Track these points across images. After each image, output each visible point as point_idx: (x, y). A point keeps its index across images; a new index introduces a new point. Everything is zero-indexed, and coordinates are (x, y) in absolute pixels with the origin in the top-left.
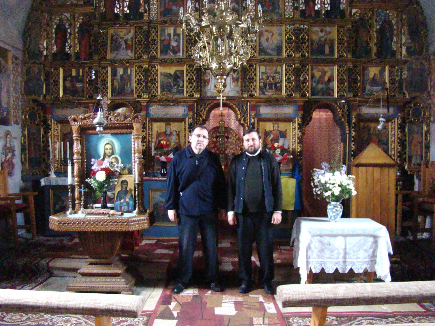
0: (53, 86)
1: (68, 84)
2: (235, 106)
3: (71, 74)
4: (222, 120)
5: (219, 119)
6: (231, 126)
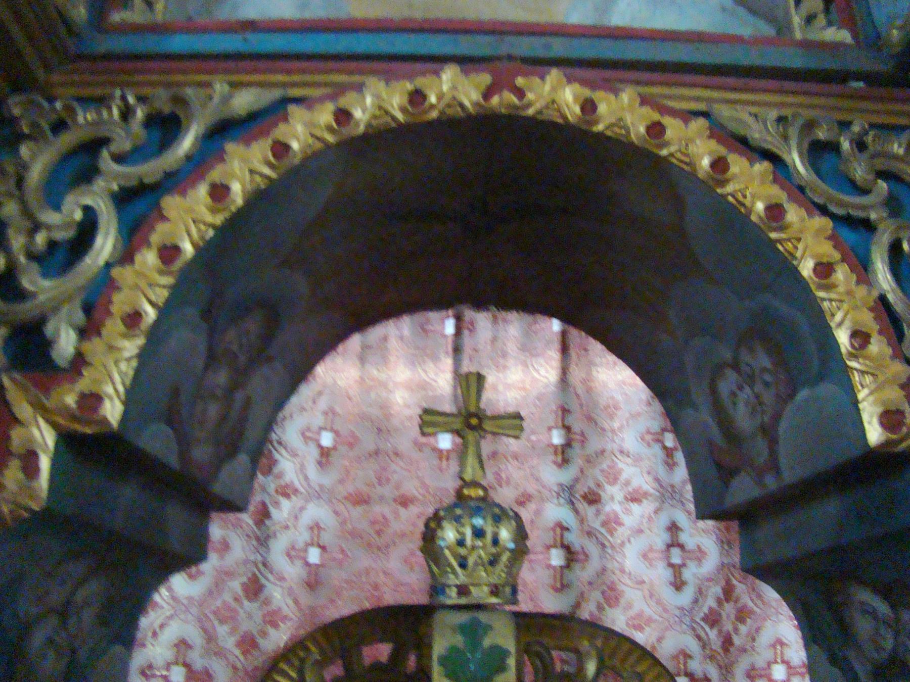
2: (751, 187)
4: (469, 501)
5: (429, 474)
6: (611, 596)
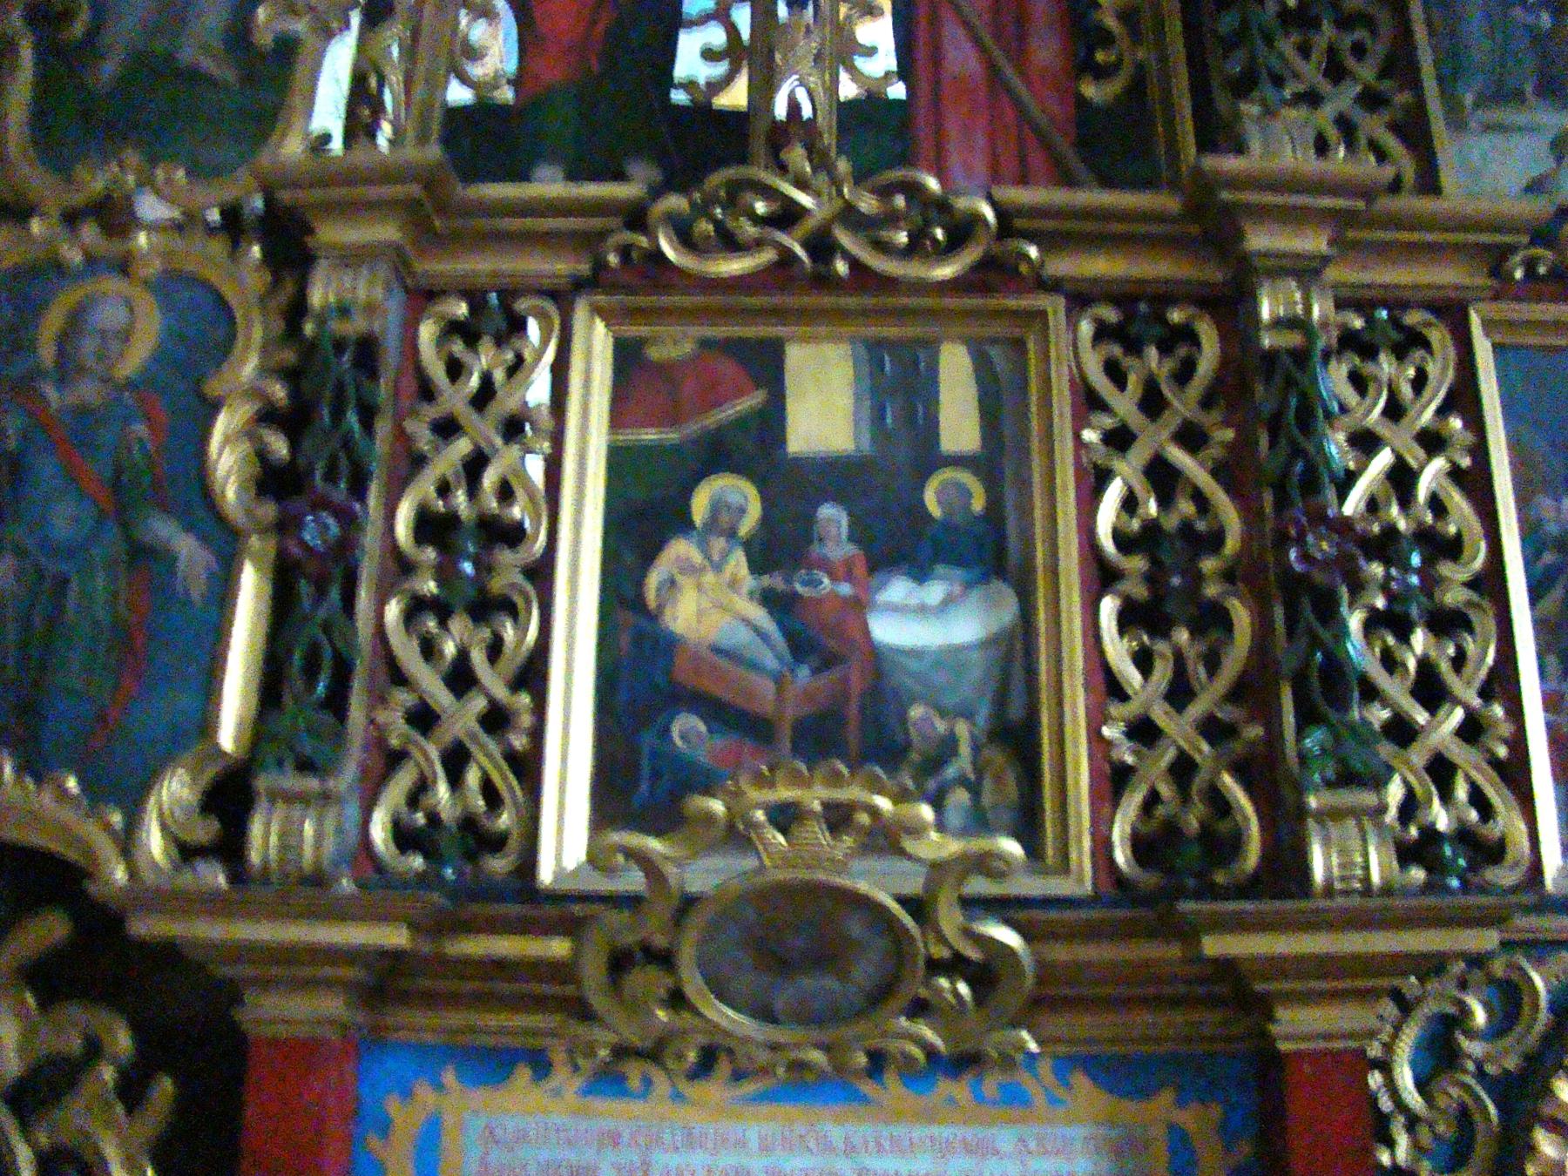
0: (416, 607)
1: (710, 602)
3: (772, 420)
